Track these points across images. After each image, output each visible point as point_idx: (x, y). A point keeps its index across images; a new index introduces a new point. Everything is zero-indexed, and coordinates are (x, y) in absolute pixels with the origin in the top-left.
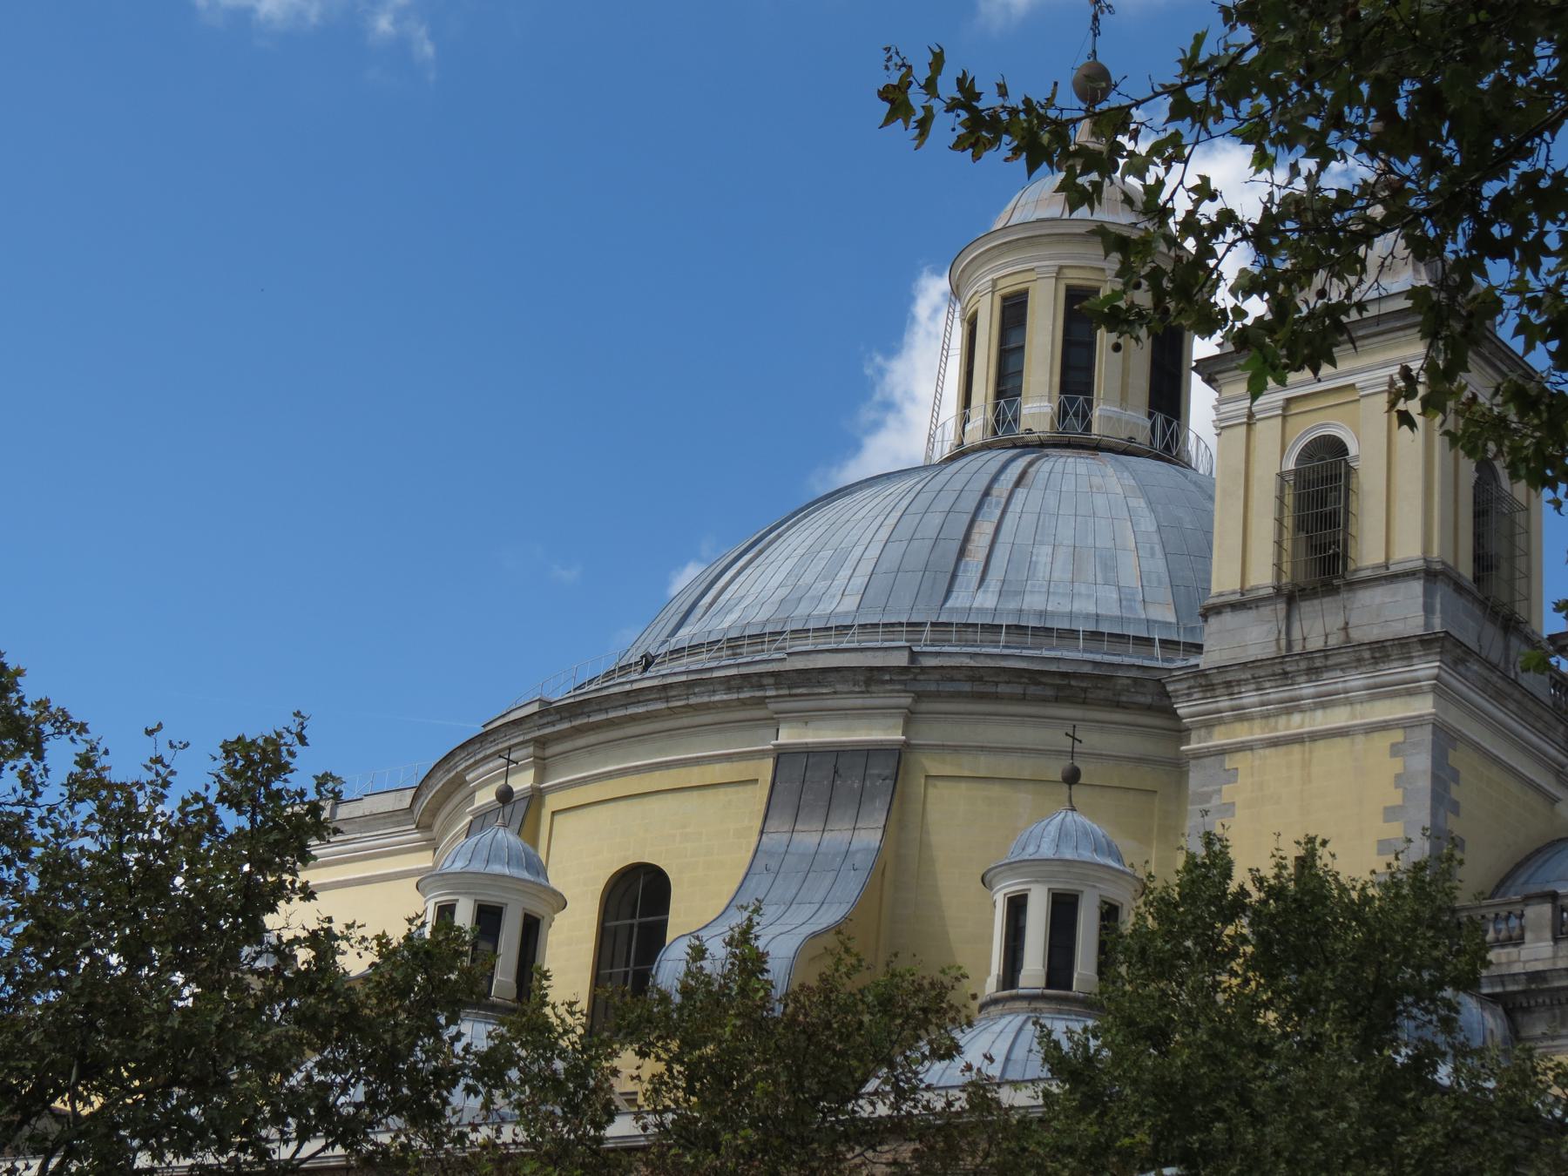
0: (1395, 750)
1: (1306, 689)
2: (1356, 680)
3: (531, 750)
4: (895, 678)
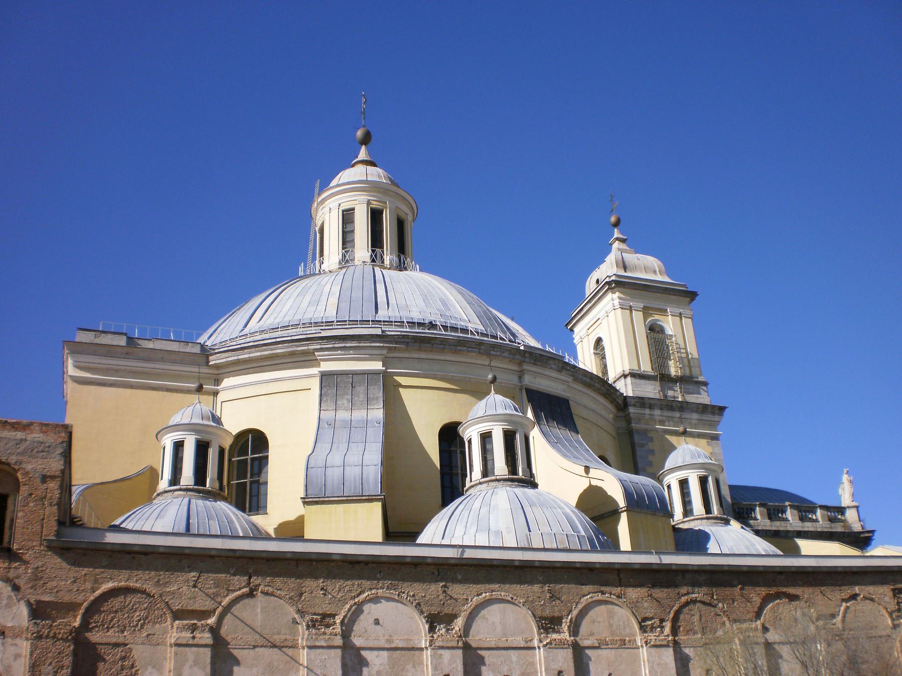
0: (709, 444)
1: (677, 414)
2: (695, 416)
3: (385, 352)
4: (571, 370)
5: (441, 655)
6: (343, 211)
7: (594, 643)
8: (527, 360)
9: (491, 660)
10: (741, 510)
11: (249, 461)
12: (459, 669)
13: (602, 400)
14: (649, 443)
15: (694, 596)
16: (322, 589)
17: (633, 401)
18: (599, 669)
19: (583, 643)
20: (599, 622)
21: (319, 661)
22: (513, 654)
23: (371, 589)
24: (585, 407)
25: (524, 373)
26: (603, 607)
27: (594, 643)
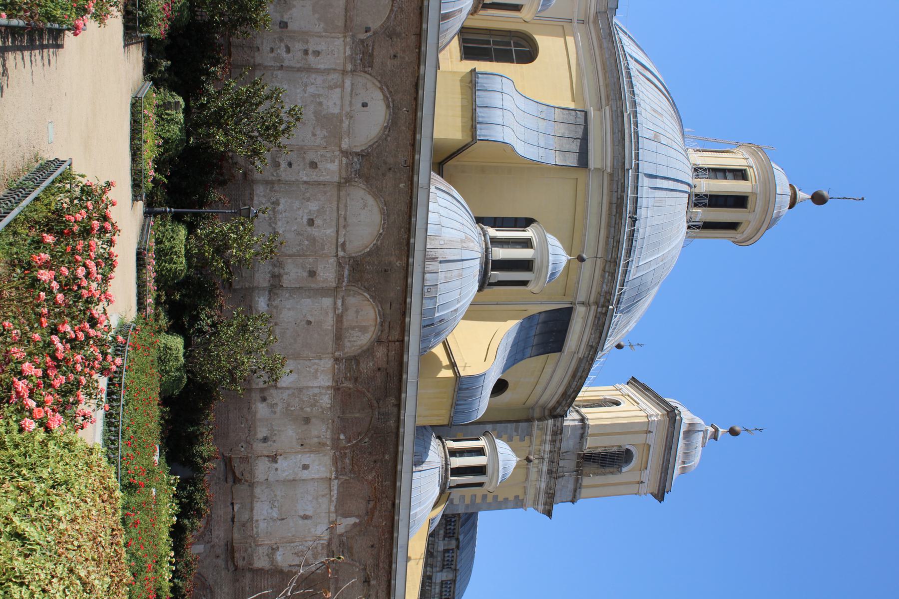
1: (545, 468)
2: (543, 485)
3: (609, 170)
5: (334, 162)
6: (745, 170)
7: (339, 309)
8: (599, 310)
9: (328, 209)
10: (453, 524)
11: (508, 48)
12: (321, 178)
13: (561, 390)
14: (519, 437)
15: (377, 413)
16: (395, 56)
17: (559, 424)
18: (315, 312)
19: (339, 299)
20: (357, 317)
21: (333, 48)
22: (330, 232)
23: (393, 101)
24: (554, 371)
25: (587, 306)
26: (373, 324)
27: (339, 309)
